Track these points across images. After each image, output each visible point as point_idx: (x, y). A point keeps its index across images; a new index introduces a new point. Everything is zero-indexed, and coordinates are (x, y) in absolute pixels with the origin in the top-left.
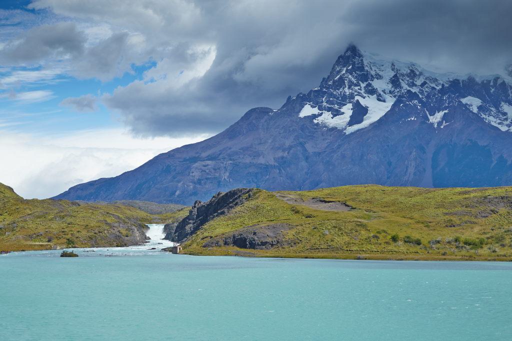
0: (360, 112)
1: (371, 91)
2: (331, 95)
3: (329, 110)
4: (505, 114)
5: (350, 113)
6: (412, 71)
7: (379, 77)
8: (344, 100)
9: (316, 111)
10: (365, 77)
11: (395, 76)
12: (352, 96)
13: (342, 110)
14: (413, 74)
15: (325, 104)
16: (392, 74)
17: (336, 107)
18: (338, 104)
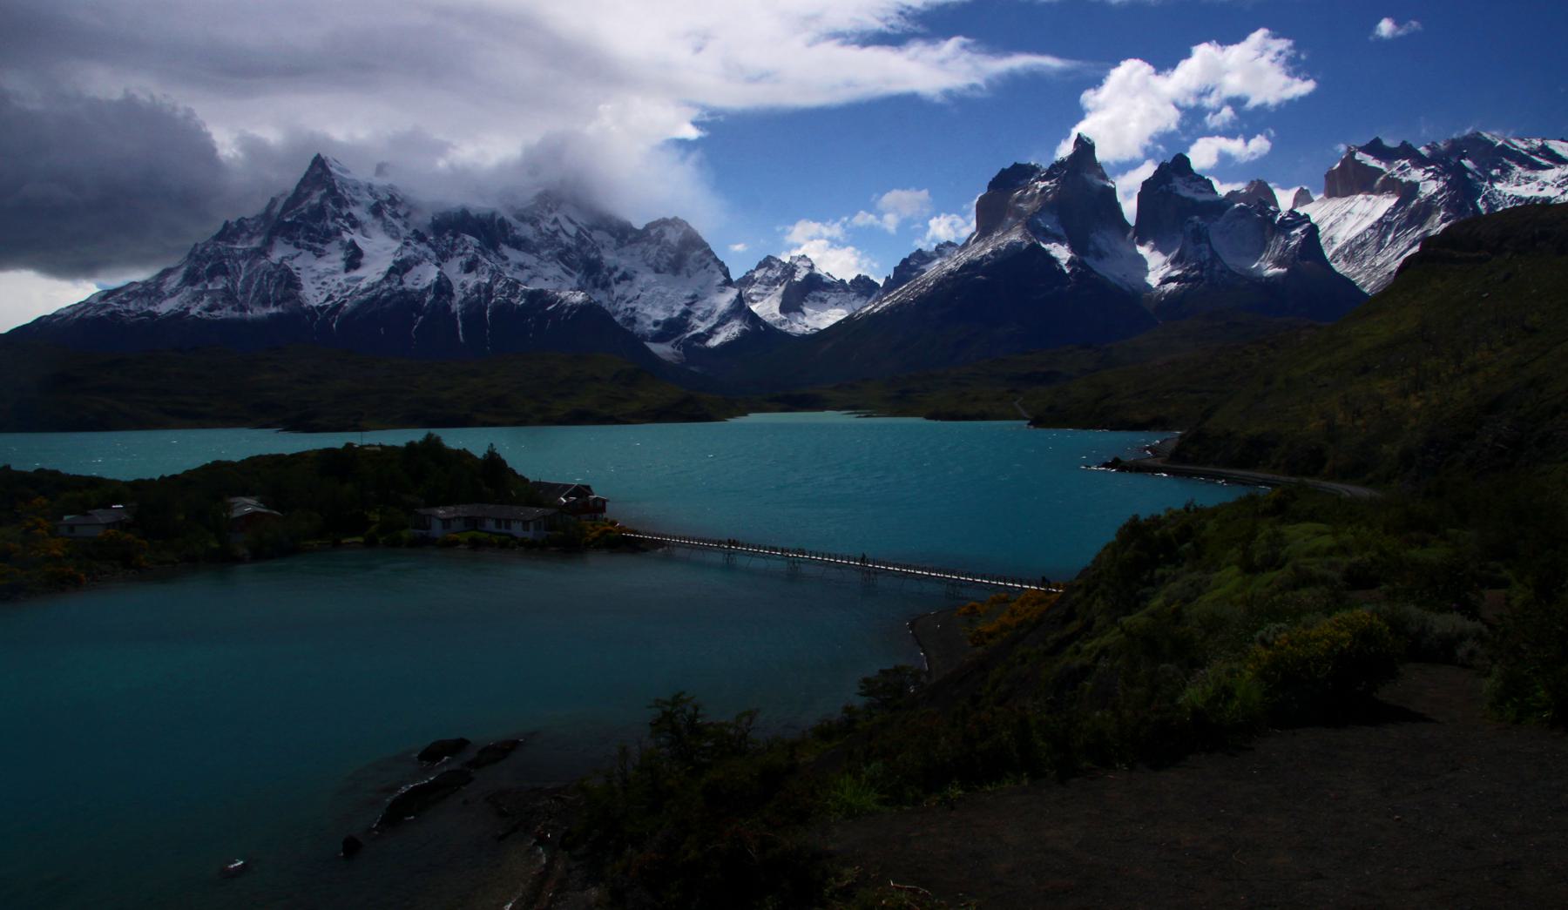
0: (354, 258)
1: (355, 224)
2: (310, 229)
3: (310, 248)
4: (505, 258)
5: (342, 255)
6: (392, 197)
7: (355, 203)
8: (329, 236)
9: (291, 250)
10: (340, 202)
11: (377, 204)
12: (339, 233)
13: (327, 248)
14: (393, 201)
15: (301, 241)
16: (372, 201)
17: (318, 245)
18: (322, 242)
